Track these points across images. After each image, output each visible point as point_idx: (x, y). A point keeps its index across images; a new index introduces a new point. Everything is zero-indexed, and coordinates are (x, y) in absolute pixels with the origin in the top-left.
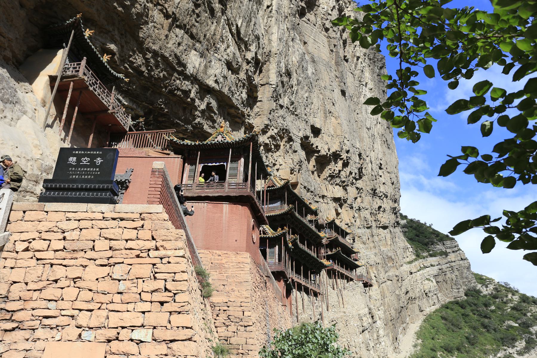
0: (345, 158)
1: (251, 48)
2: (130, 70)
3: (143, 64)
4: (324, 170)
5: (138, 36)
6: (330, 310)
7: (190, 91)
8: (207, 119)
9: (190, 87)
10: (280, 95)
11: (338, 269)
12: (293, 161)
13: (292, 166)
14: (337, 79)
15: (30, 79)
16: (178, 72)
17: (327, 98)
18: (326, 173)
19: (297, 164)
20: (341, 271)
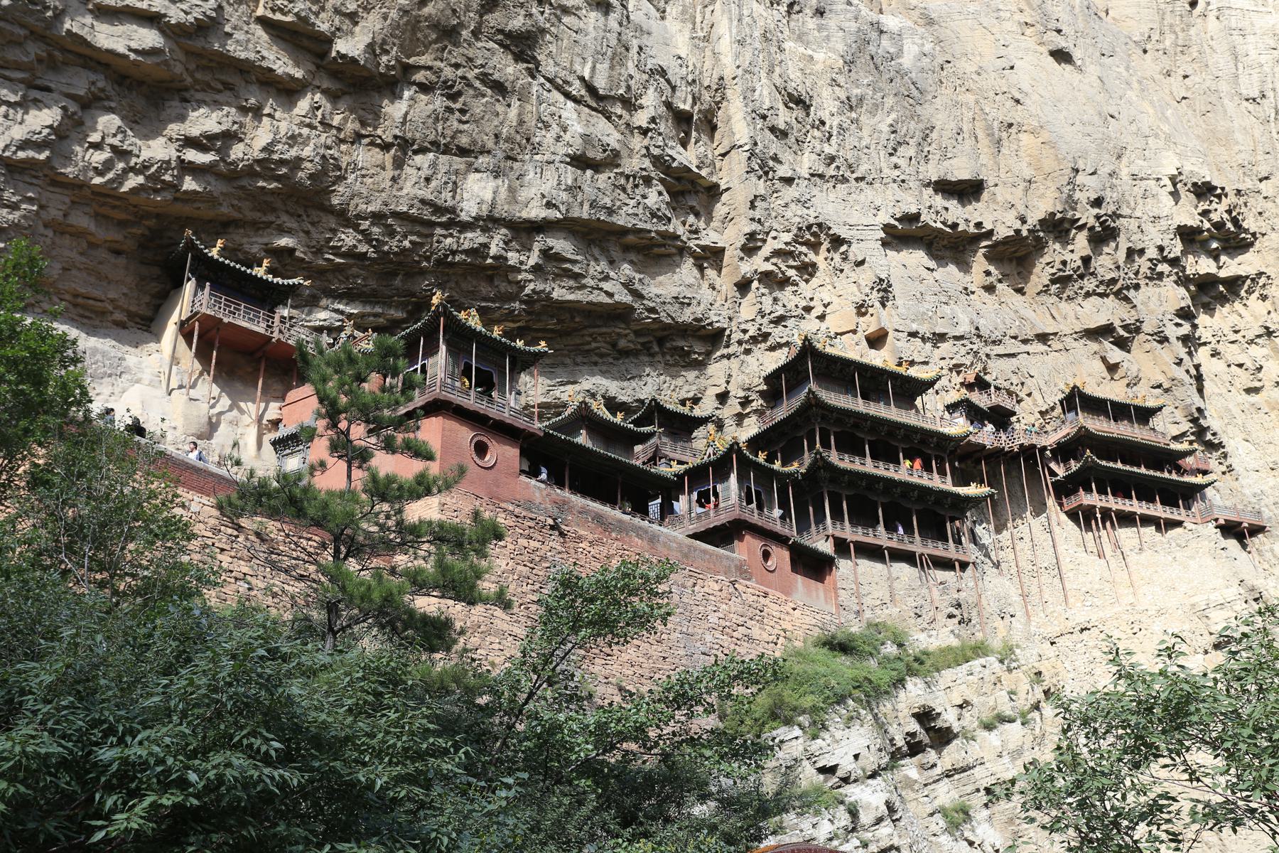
0: (1091, 221)
1: (642, 101)
2: (338, 260)
3: (360, 241)
4: (1031, 273)
5: (331, 205)
6: (1079, 604)
7: (486, 246)
8: (557, 277)
9: (483, 239)
10: (775, 158)
11: (1099, 504)
12: (859, 286)
13: (859, 298)
14: (1029, 31)
15: (158, 337)
16: (441, 225)
17: (991, 94)
18: (1041, 274)
19: (873, 288)
20: (1114, 507)
